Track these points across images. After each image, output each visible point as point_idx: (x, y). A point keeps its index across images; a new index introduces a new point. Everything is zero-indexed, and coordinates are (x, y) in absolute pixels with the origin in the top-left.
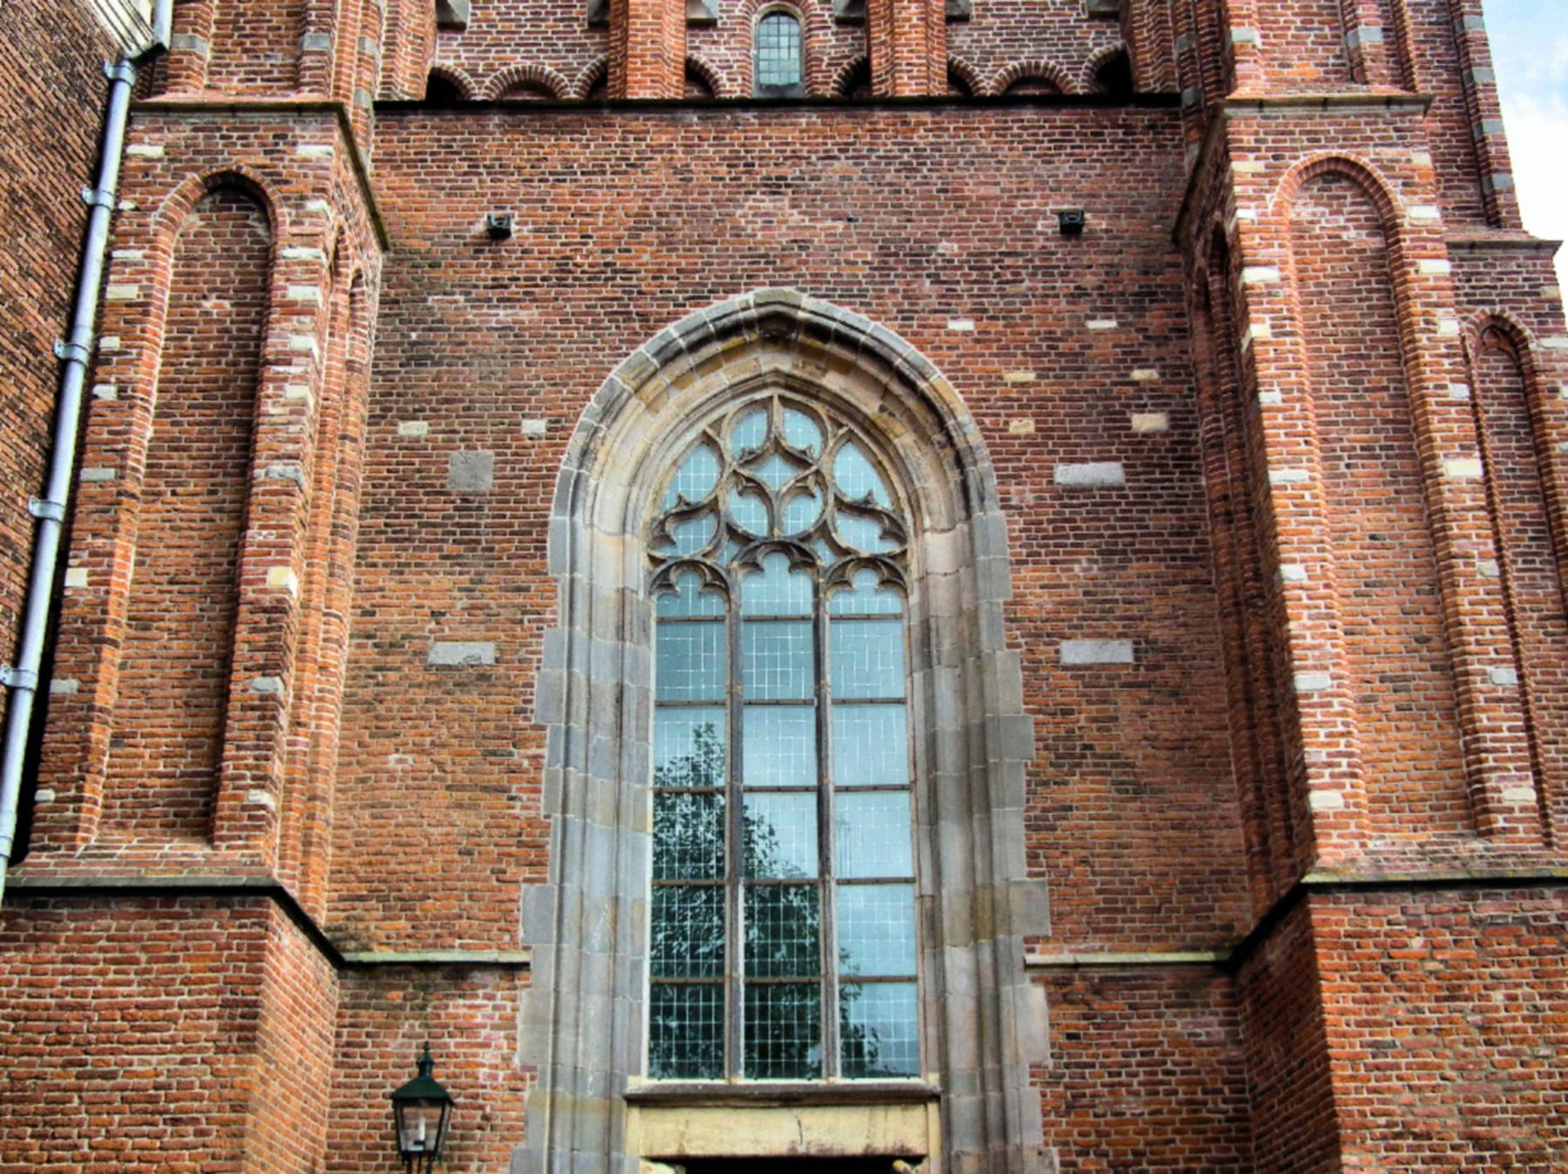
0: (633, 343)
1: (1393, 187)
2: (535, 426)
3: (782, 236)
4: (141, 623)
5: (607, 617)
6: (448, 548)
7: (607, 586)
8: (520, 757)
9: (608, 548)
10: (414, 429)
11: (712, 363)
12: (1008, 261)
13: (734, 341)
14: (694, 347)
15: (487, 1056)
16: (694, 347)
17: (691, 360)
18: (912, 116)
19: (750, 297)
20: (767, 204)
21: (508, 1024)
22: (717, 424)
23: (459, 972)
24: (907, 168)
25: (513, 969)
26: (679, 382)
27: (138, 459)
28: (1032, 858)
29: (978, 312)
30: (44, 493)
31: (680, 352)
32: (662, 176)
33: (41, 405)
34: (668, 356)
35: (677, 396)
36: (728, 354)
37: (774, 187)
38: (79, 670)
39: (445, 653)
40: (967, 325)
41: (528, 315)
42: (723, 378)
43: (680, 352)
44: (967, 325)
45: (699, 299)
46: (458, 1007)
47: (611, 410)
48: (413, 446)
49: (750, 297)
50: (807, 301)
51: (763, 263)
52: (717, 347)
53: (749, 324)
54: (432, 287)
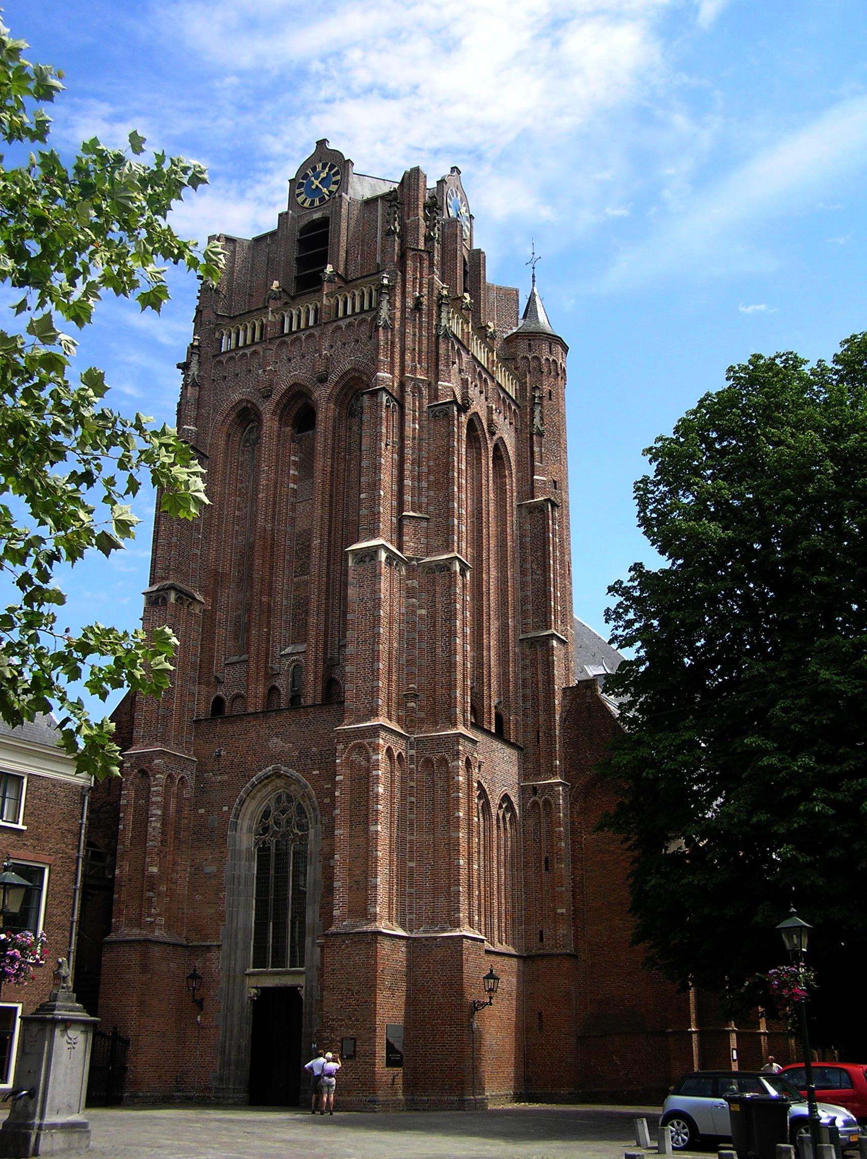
0: (246, 784)
1: (370, 750)
2: (225, 809)
3: (279, 750)
4: (130, 880)
5: (244, 855)
6: (208, 843)
7: (244, 847)
8: (221, 895)
9: (244, 838)
10: (202, 811)
11: (265, 786)
12: (327, 752)
13: (270, 779)
14: (260, 783)
15: (214, 966)
16: (260, 783)
17: (260, 786)
18: (309, 710)
19: (270, 768)
20: (275, 740)
21: (218, 958)
22: (269, 800)
23: (209, 948)
24: (307, 726)
25: (219, 946)
26: (259, 791)
27: (128, 843)
28: (320, 916)
29: (319, 769)
30: (76, 884)
31: (256, 785)
32: (253, 735)
33: (74, 868)
34: (254, 786)
35: (259, 794)
36: (270, 782)
37: (277, 735)
38: (118, 893)
39: (208, 869)
40: (317, 772)
41: (226, 777)
42: (269, 788)
43: (256, 785)
44: (317, 772)
45: (260, 770)
46: (209, 955)
47: (242, 803)
48: (201, 816)
49: (270, 768)
50: (283, 768)
51: (273, 758)
52: (266, 781)
53: (272, 775)
54: (206, 771)
